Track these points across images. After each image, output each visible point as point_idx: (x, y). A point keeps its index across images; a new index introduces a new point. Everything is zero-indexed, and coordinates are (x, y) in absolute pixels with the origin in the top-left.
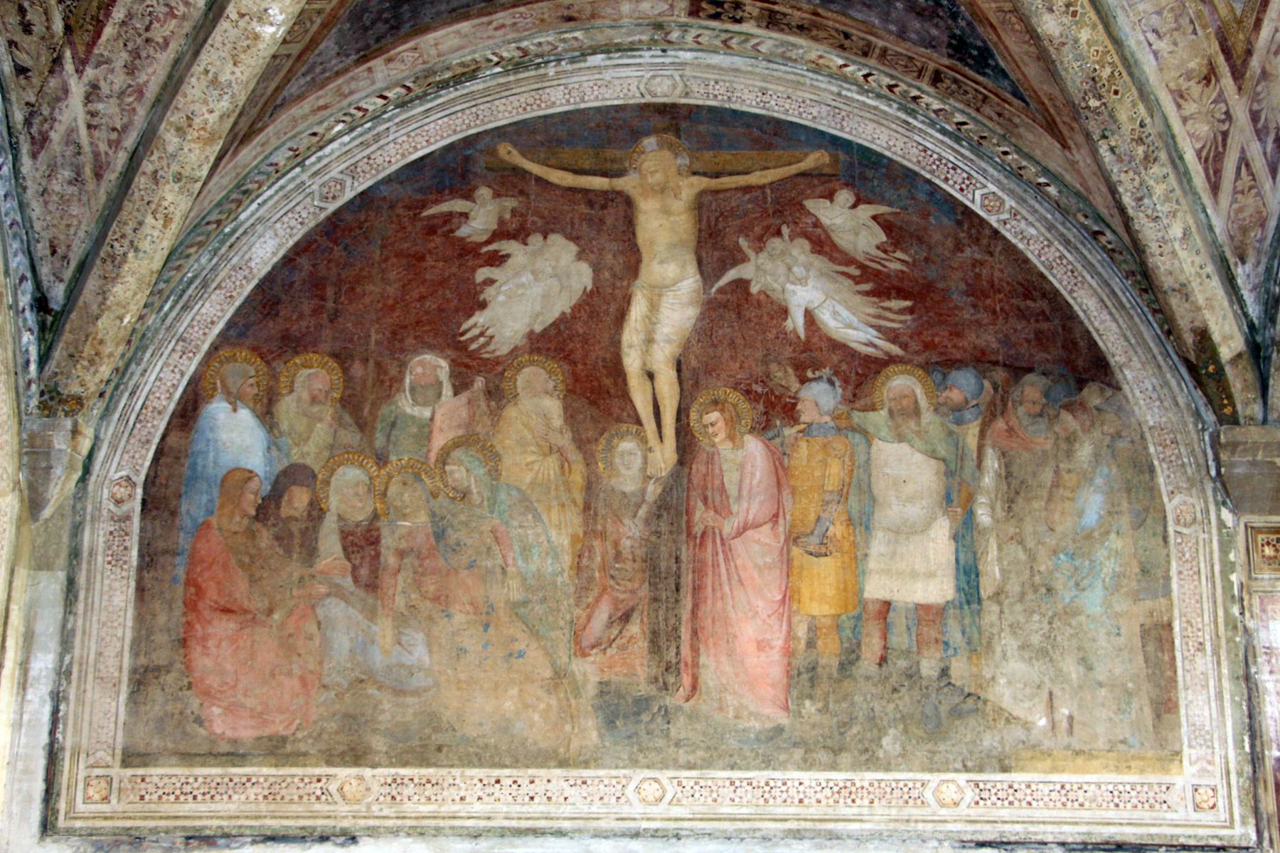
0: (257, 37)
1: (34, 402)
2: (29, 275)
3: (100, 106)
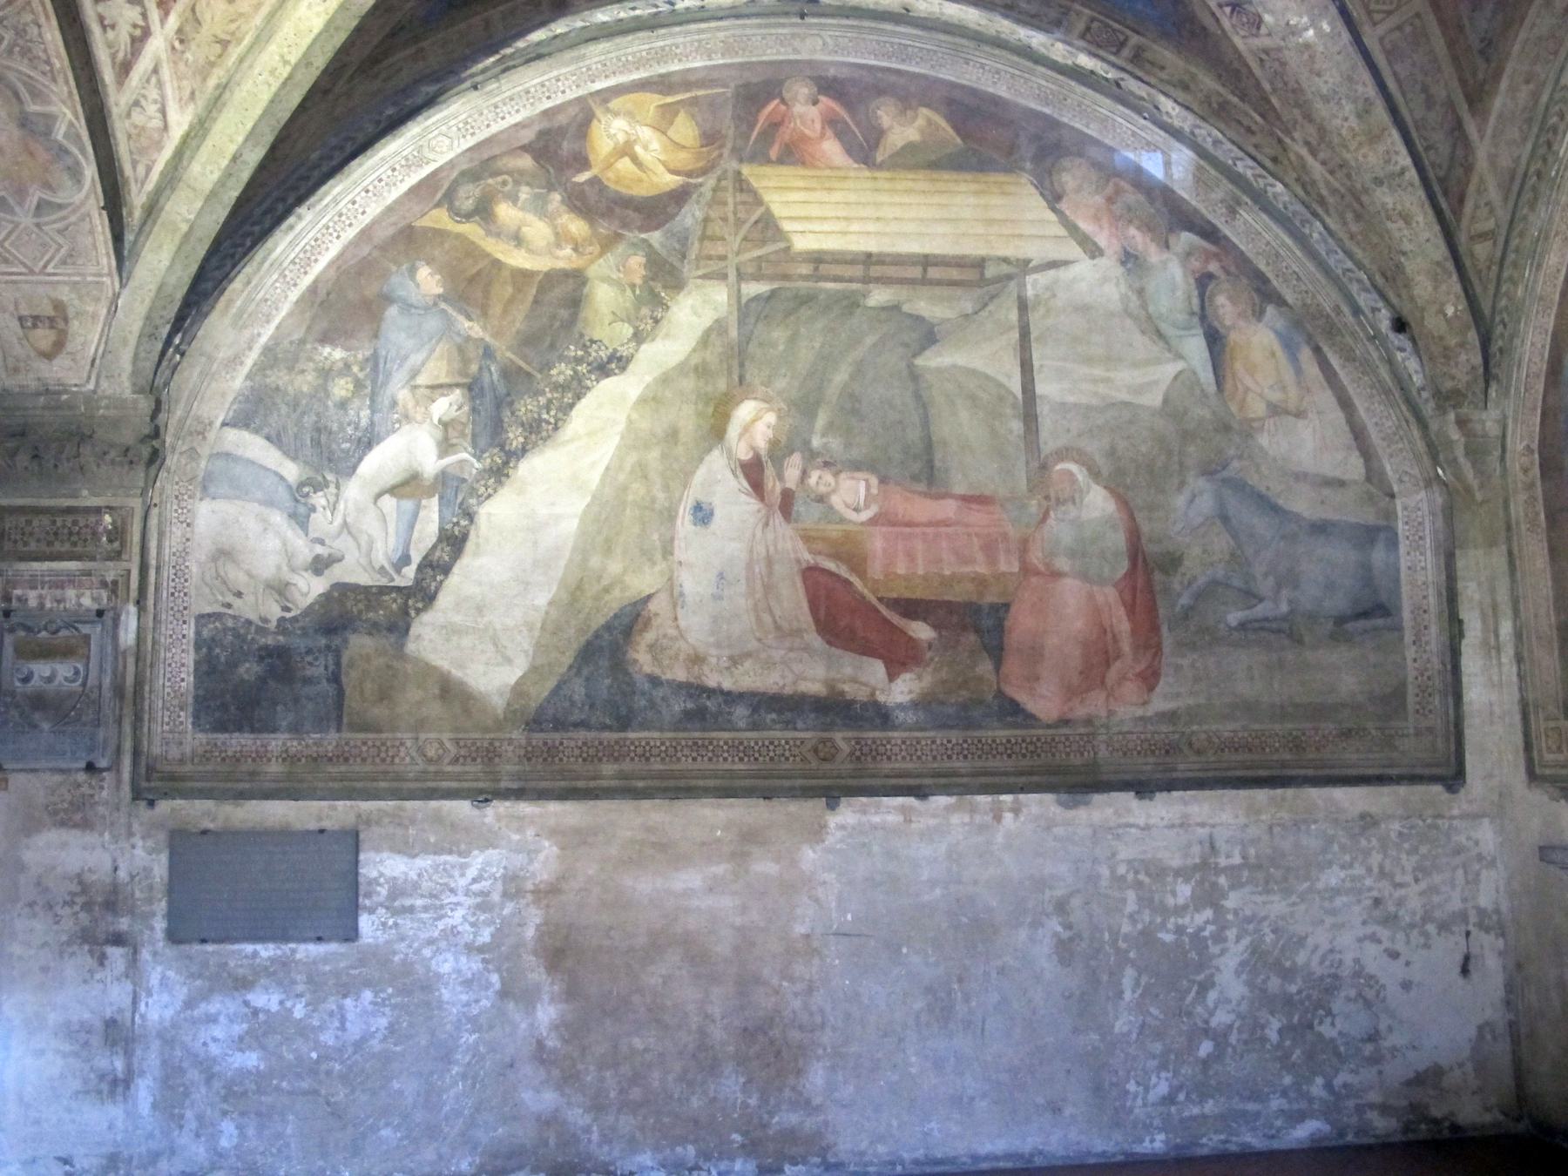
0: (1307, 46)
1: (1431, 404)
2: (1380, 304)
3: (1322, 155)
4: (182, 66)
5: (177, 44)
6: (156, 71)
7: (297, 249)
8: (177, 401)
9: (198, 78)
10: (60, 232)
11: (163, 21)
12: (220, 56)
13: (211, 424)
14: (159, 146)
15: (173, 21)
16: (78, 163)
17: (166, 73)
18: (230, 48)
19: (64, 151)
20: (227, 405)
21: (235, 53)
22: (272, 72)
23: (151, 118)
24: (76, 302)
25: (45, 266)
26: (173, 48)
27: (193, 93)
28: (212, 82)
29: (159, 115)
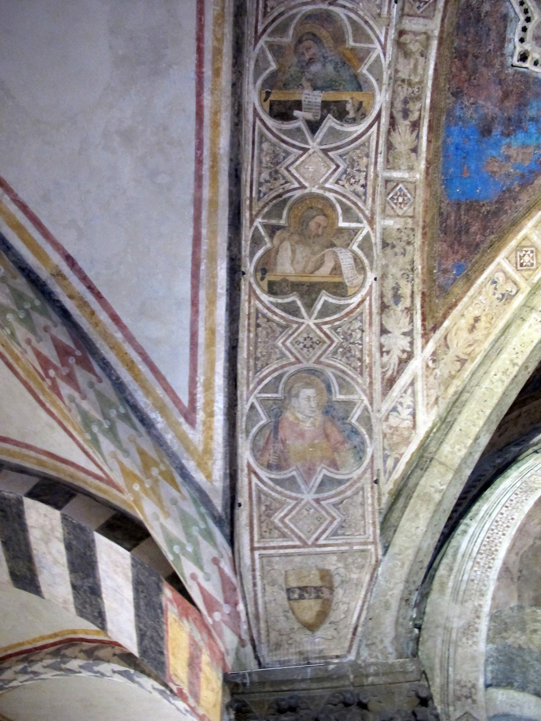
4: (431, 379)
5: (430, 363)
6: (412, 384)
7: (478, 544)
8: (432, 669)
9: (442, 388)
10: (335, 505)
11: (423, 348)
12: (459, 371)
13: (474, 686)
14: (407, 441)
15: (431, 347)
16: (363, 443)
17: (419, 385)
18: (466, 365)
19: (355, 432)
20: (482, 668)
21: (470, 367)
22: (505, 373)
23: (404, 420)
24: (342, 571)
25: (317, 539)
26: (427, 366)
27: (437, 399)
28: (451, 390)
29: (410, 417)
